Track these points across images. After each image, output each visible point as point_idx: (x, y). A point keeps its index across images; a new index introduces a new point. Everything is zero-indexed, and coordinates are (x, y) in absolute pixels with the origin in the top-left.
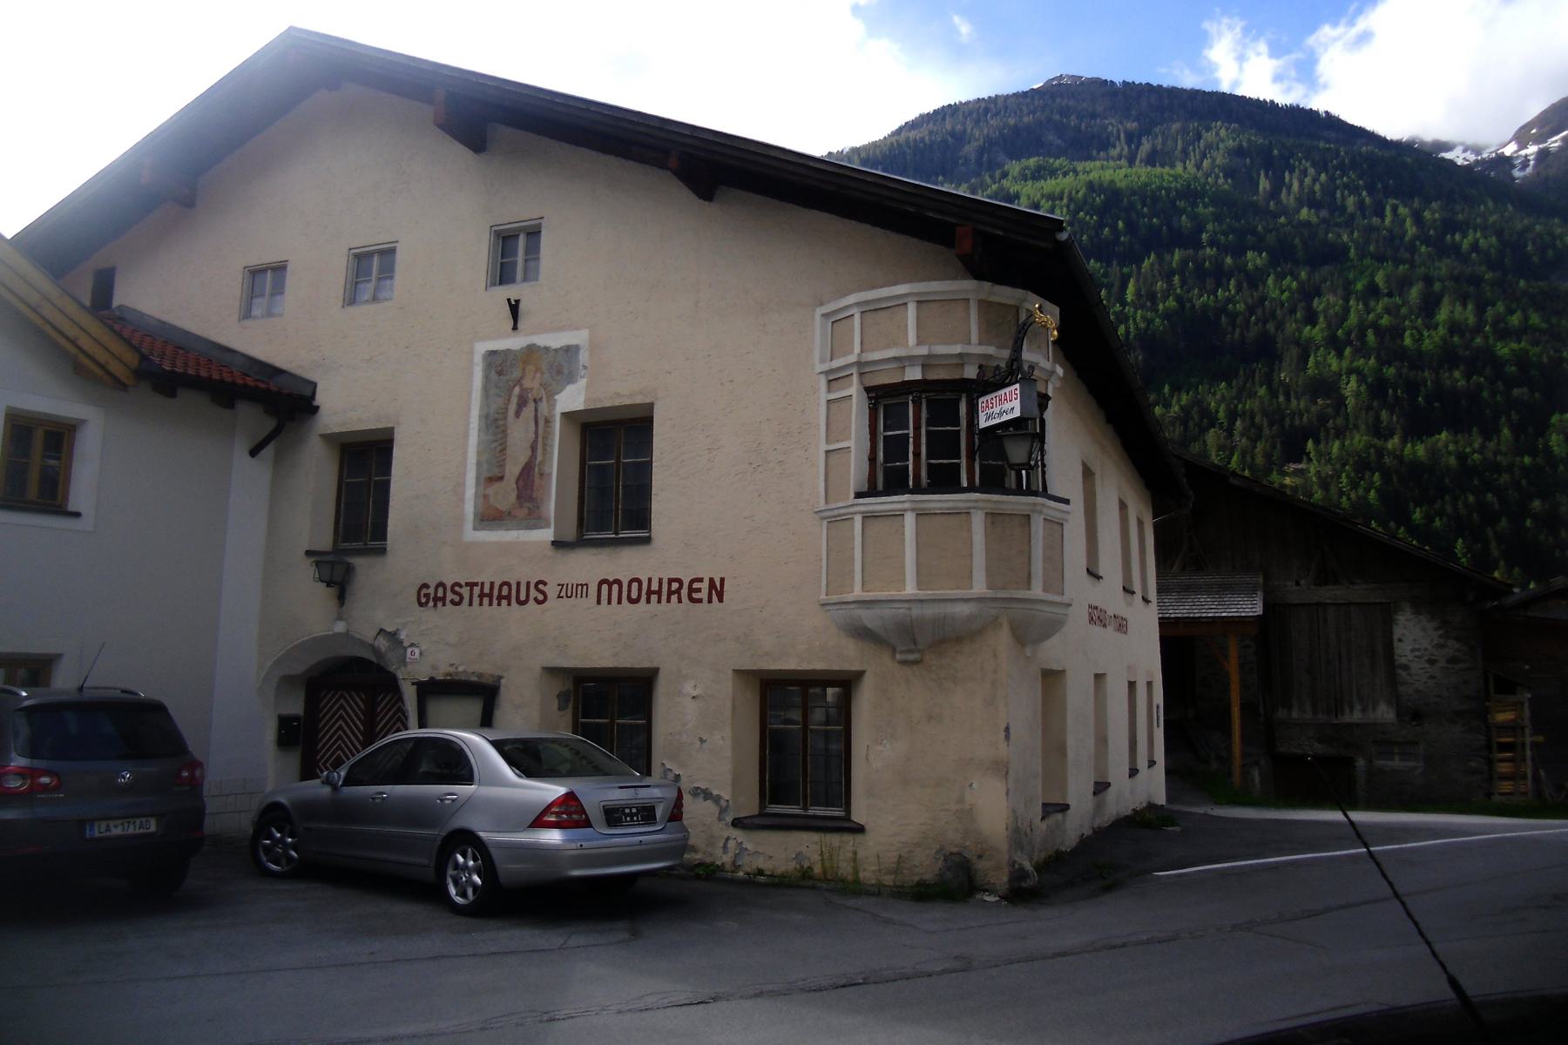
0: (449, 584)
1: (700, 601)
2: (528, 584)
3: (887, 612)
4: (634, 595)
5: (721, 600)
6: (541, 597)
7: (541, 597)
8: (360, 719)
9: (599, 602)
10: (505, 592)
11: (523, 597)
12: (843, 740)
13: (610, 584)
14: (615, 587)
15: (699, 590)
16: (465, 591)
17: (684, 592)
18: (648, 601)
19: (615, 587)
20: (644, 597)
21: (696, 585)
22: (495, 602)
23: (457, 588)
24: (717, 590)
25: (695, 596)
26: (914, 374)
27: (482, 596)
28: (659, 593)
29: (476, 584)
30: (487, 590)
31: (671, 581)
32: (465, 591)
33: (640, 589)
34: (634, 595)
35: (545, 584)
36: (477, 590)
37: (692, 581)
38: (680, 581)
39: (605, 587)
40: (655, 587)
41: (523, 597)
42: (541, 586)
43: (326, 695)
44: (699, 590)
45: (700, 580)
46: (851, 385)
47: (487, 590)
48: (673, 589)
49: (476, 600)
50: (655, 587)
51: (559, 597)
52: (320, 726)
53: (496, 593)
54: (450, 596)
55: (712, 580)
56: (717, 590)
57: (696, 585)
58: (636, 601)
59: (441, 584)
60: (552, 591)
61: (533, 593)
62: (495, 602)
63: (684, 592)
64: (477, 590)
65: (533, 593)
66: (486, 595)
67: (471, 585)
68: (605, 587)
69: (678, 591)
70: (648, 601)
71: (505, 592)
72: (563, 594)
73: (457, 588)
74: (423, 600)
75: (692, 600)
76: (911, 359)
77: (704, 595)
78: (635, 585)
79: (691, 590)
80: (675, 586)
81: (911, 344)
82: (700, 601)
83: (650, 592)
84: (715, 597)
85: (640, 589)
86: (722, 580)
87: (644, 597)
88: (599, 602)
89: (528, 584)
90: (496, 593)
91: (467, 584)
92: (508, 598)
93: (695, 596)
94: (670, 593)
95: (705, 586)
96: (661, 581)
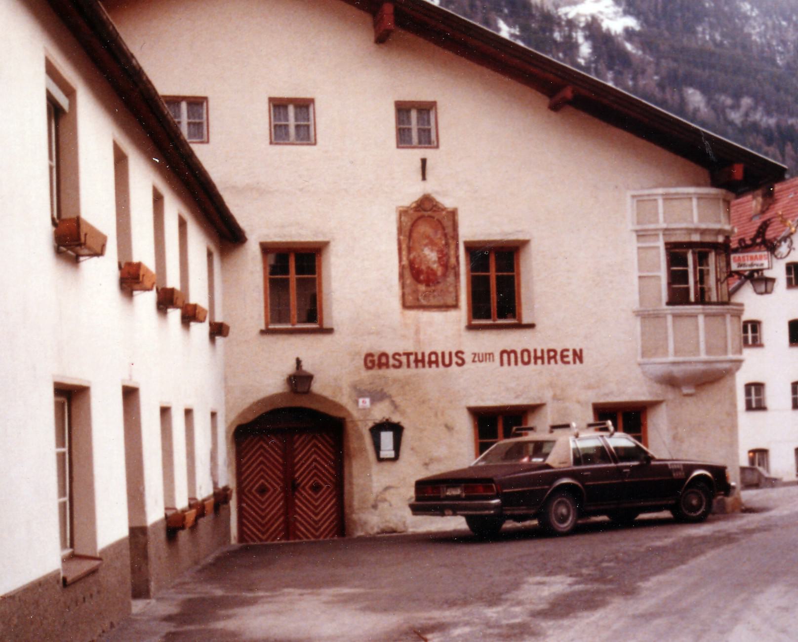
0: (390, 353)
1: (568, 363)
2: (450, 354)
3: (683, 367)
4: (526, 359)
5: (581, 361)
6: (460, 362)
7: (460, 362)
8: (330, 452)
9: (502, 364)
10: (433, 358)
11: (447, 361)
12: (526, 432)
13: (509, 353)
14: (512, 356)
15: (567, 356)
16: (404, 359)
17: (558, 357)
19: (512, 356)
20: (532, 360)
21: (565, 353)
22: (427, 365)
23: (397, 357)
24: (578, 356)
25: (566, 359)
26: (696, 238)
27: (416, 361)
28: (542, 358)
29: (411, 354)
30: (420, 357)
31: (549, 351)
32: (404, 359)
33: (529, 356)
34: (526, 359)
35: (462, 353)
36: (412, 358)
37: (562, 352)
38: (555, 351)
39: (505, 356)
41: (447, 361)
42: (460, 355)
43: (298, 439)
44: (567, 356)
45: (567, 350)
46: (658, 240)
47: (420, 357)
48: (551, 356)
49: (413, 364)
51: (474, 361)
52: (296, 460)
53: (427, 359)
54: (391, 361)
55: (575, 352)
56: (578, 356)
57: (565, 353)
58: (528, 363)
59: (384, 354)
60: (468, 357)
61: (455, 359)
62: (427, 365)
63: (558, 357)
64: (412, 358)
65: (455, 359)
66: (420, 361)
67: (408, 355)
68: (505, 356)
69: (554, 357)
70: (536, 363)
72: (476, 359)
73: (397, 357)
74: (370, 365)
76: (696, 230)
77: (570, 359)
78: (526, 354)
79: (562, 357)
80: (552, 354)
81: (695, 221)
82: (568, 363)
83: (536, 358)
84: (577, 361)
85: (529, 356)
86: (581, 351)
87: (532, 360)
89: (450, 354)
90: (427, 359)
91: (405, 354)
92: (436, 362)
93: (566, 359)
94: (549, 358)
95: (570, 353)
96: (542, 351)
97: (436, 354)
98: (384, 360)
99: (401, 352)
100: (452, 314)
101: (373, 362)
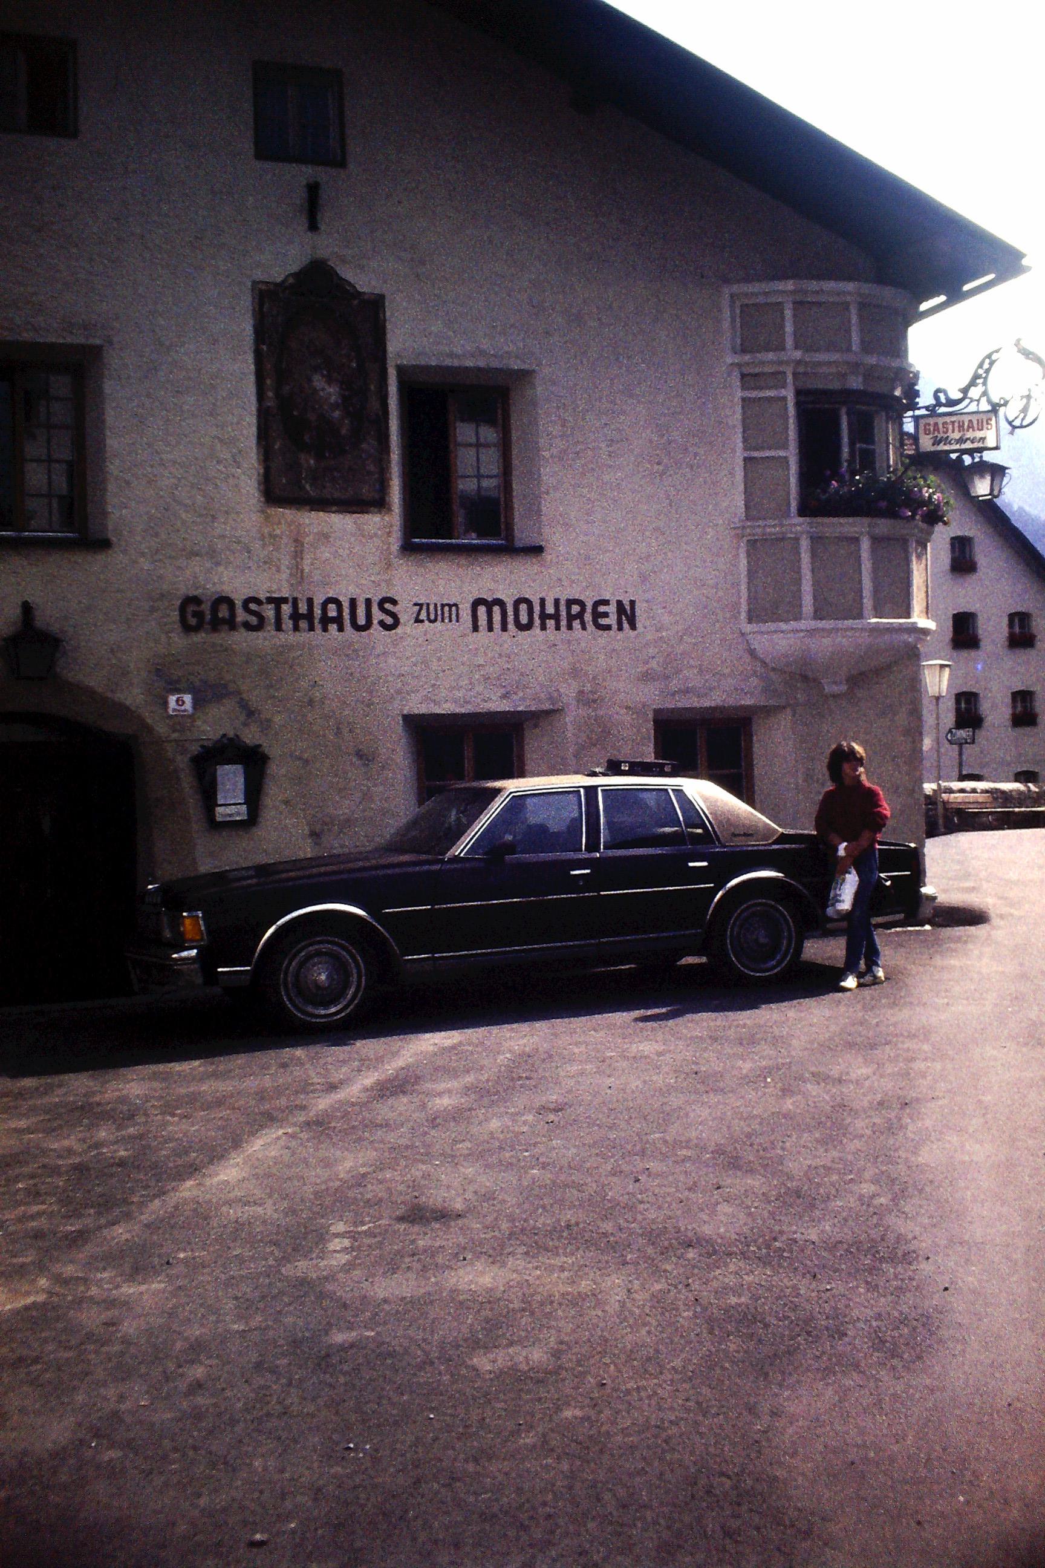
1: (608, 628)
2: (368, 602)
4: (524, 619)
5: (633, 627)
6: (389, 621)
7: (389, 621)
9: (476, 628)
11: (361, 621)
13: (489, 605)
14: (496, 609)
15: (606, 615)
16: (269, 612)
17: (588, 617)
18: (543, 627)
20: (537, 622)
21: (602, 609)
23: (253, 606)
24: (627, 614)
25: (603, 621)
27: (296, 616)
28: (556, 617)
29: (284, 600)
30: (303, 608)
31: (570, 603)
32: (269, 612)
34: (524, 619)
35: (394, 602)
36: (286, 609)
37: (597, 604)
38: (581, 604)
39: (482, 610)
40: (550, 610)
41: (361, 621)
42: (387, 606)
44: (606, 615)
45: (606, 602)
47: (303, 608)
49: (288, 624)
50: (550, 610)
51: (418, 620)
53: (318, 612)
54: (241, 616)
55: (620, 603)
56: (627, 614)
57: (602, 609)
58: (528, 626)
60: (405, 611)
61: (377, 615)
63: (588, 617)
65: (377, 615)
67: (278, 602)
68: (482, 610)
69: (580, 616)
70: (543, 627)
71: (332, 612)
72: (423, 616)
73: (253, 606)
74: (193, 621)
75: (600, 627)
77: (612, 620)
78: (523, 607)
79: (597, 615)
80: (576, 609)
82: (608, 628)
83: (544, 617)
84: (626, 625)
86: (632, 603)
87: (537, 622)
88: (476, 628)
89: (368, 602)
90: (318, 612)
91: (270, 600)
92: (339, 620)
93: (603, 621)
94: (571, 618)
95: (612, 609)
96: (557, 602)
97: (335, 601)
98: (223, 612)
99: (262, 596)
100: (373, 521)
101: (199, 615)
